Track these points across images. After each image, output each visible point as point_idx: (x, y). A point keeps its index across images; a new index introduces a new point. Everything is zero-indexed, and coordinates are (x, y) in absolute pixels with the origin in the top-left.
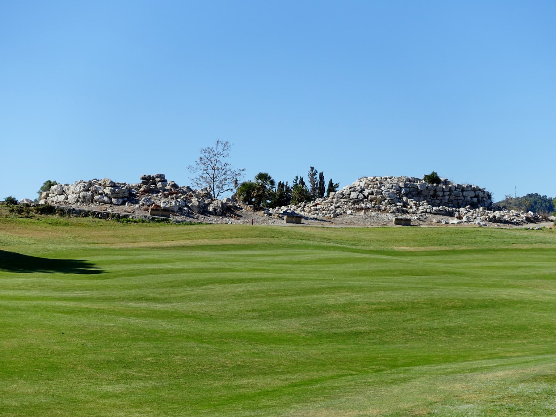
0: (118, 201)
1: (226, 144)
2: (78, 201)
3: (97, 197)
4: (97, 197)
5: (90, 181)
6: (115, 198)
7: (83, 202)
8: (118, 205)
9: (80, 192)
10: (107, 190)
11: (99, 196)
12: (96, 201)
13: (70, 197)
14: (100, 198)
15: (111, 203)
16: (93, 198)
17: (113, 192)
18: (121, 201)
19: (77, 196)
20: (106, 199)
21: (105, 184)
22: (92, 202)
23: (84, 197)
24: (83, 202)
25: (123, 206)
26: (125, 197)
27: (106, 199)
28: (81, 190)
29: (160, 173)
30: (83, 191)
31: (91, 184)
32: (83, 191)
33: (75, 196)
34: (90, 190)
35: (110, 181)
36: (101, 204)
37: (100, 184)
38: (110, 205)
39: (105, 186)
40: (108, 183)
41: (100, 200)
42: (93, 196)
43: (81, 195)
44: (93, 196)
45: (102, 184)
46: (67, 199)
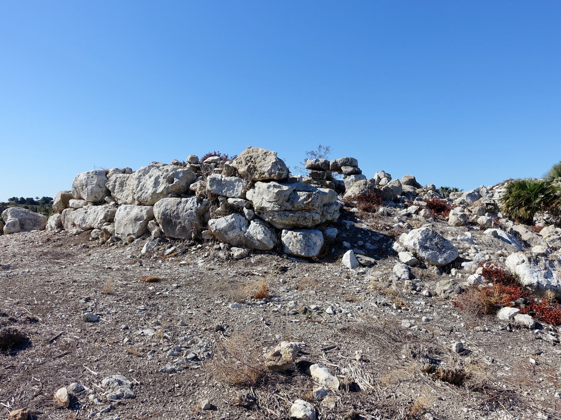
0: (307, 243)
1: (327, 149)
2: (145, 233)
3: (219, 223)
4: (219, 223)
5: (194, 159)
6: (294, 228)
7: (162, 238)
8: (310, 260)
9: (156, 196)
10: (263, 196)
11: (230, 218)
12: (216, 238)
13: (120, 213)
14: (231, 227)
15: (279, 249)
16: (205, 224)
17: (287, 203)
18: (318, 240)
19: (143, 211)
20: (255, 230)
21: (251, 170)
22: (199, 240)
23: (168, 220)
24: (162, 238)
25: (329, 267)
26: (330, 224)
27: (255, 230)
28: (160, 189)
29: (349, 157)
30: (167, 193)
31: (198, 169)
32: (167, 193)
33: (136, 211)
34: (193, 193)
35: (272, 159)
36: (236, 252)
37: (233, 172)
38: (274, 261)
39: (251, 178)
40: (266, 166)
41: (231, 235)
42: (202, 218)
43: (157, 211)
44: (202, 218)
45: (242, 169)
46: (110, 219)
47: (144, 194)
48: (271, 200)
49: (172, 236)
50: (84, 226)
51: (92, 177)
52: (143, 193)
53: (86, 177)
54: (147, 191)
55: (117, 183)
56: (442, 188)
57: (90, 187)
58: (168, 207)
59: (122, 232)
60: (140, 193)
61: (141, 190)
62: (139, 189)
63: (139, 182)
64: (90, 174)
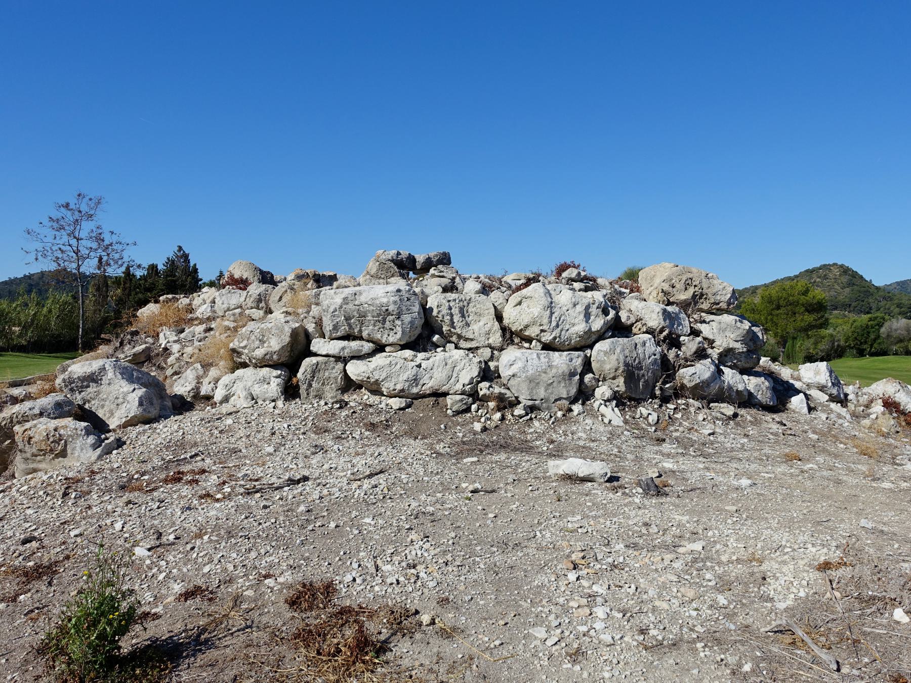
47: (563, 333)
48: (739, 339)
49: (633, 396)
50: (415, 390)
51: (408, 299)
52: (562, 330)
53: (397, 298)
54: (568, 327)
55: (455, 311)
57: (407, 318)
58: (627, 352)
59: (542, 397)
60: (556, 333)
61: (557, 326)
62: (554, 324)
63: (552, 313)
64: (403, 293)
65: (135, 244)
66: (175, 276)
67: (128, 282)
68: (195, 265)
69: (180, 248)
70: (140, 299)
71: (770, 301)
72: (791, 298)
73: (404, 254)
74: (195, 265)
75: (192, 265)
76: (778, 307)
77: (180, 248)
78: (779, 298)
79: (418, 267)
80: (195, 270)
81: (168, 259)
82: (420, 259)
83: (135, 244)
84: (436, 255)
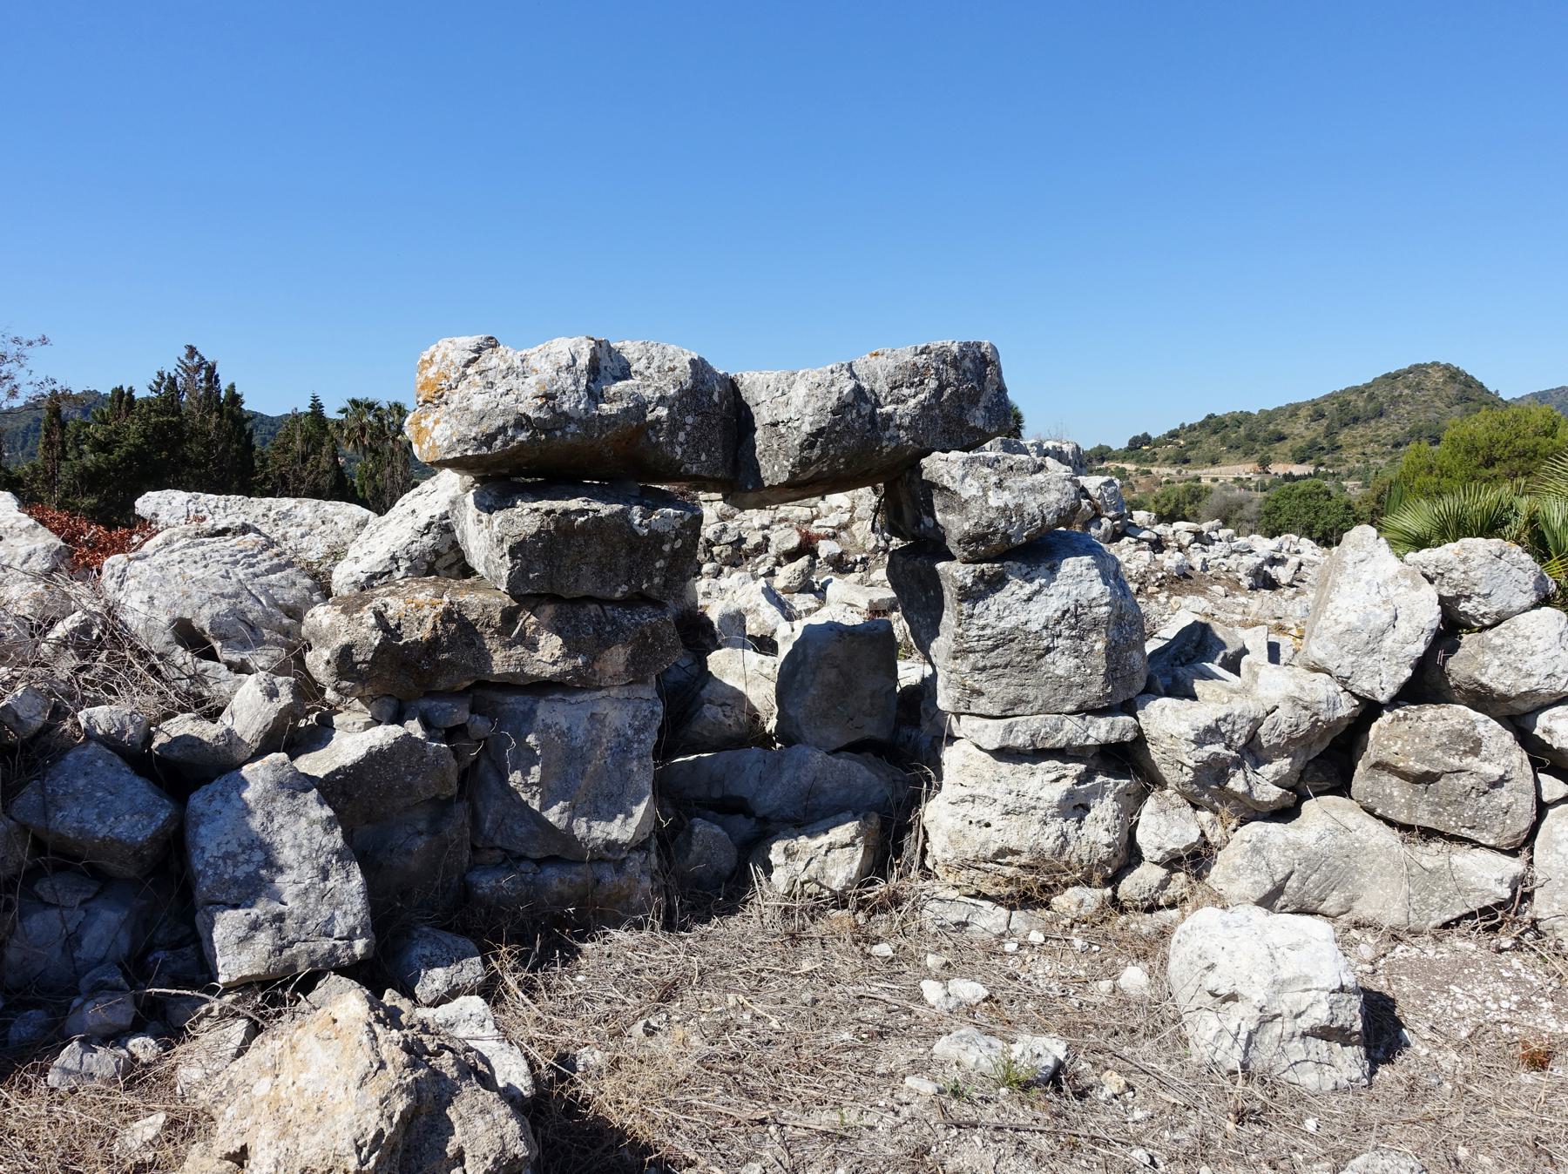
56: (354, 402)
65: (44, 341)
66: (177, 412)
67: (57, 430)
68: (233, 386)
69: (192, 351)
70: (85, 468)
71: (1472, 450)
72: (1519, 442)
73: (657, 365)
74: (233, 386)
75: (224, 386)
76: (1490, 462)
77: (192, 351)
78: (1492, 443)
79: (774, 470)
80: (235, 399)
81: (161, 375)
82: (786, 402)
83: (44, 341)
84: (916, 375)
